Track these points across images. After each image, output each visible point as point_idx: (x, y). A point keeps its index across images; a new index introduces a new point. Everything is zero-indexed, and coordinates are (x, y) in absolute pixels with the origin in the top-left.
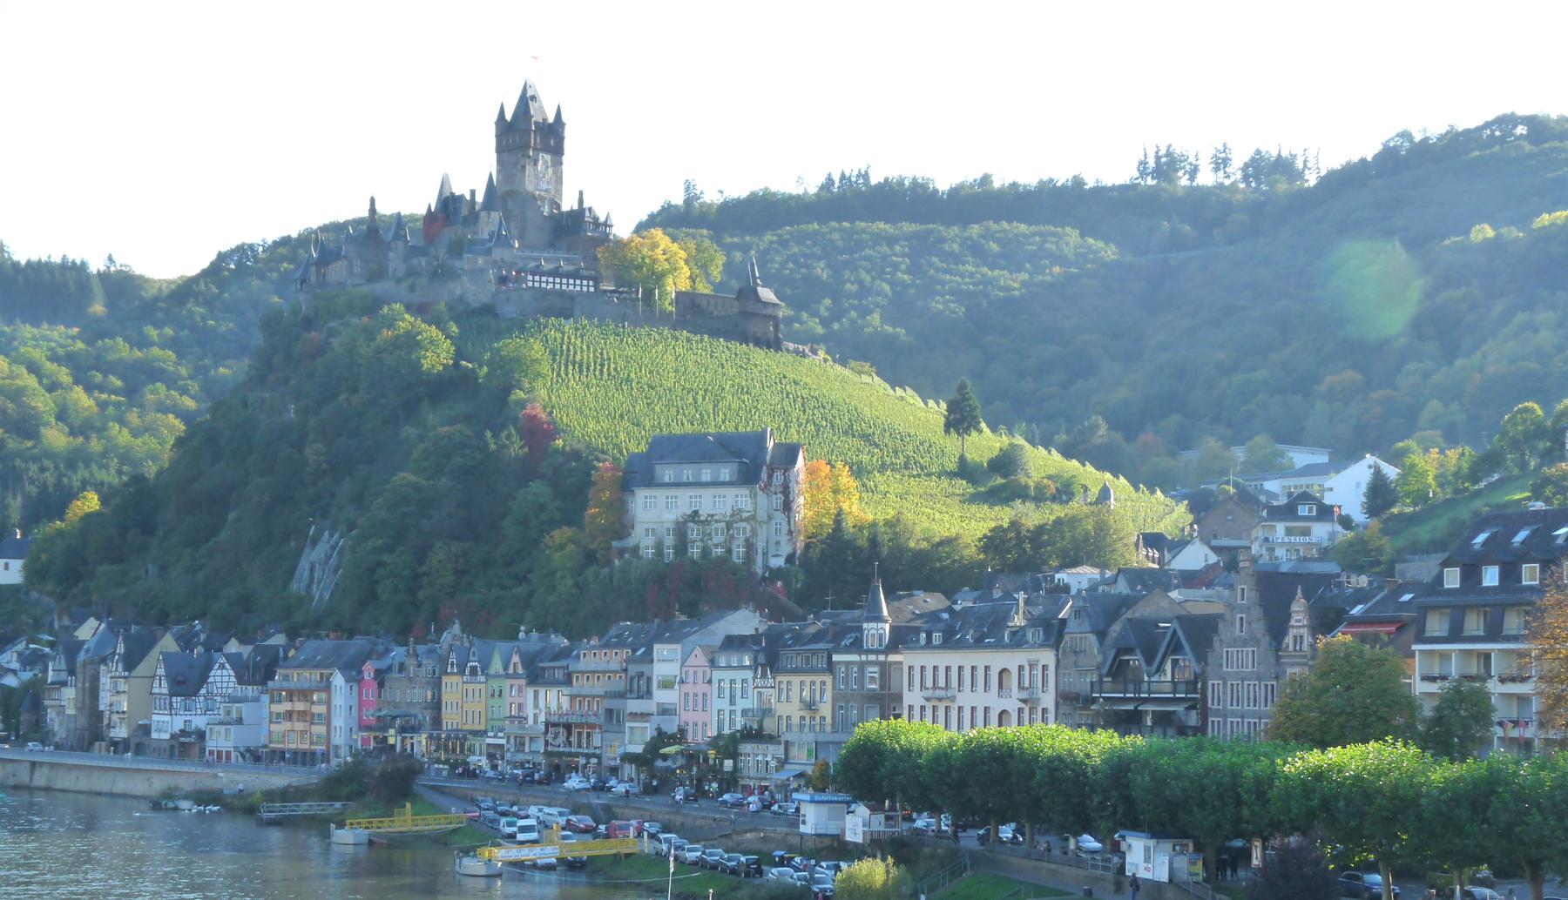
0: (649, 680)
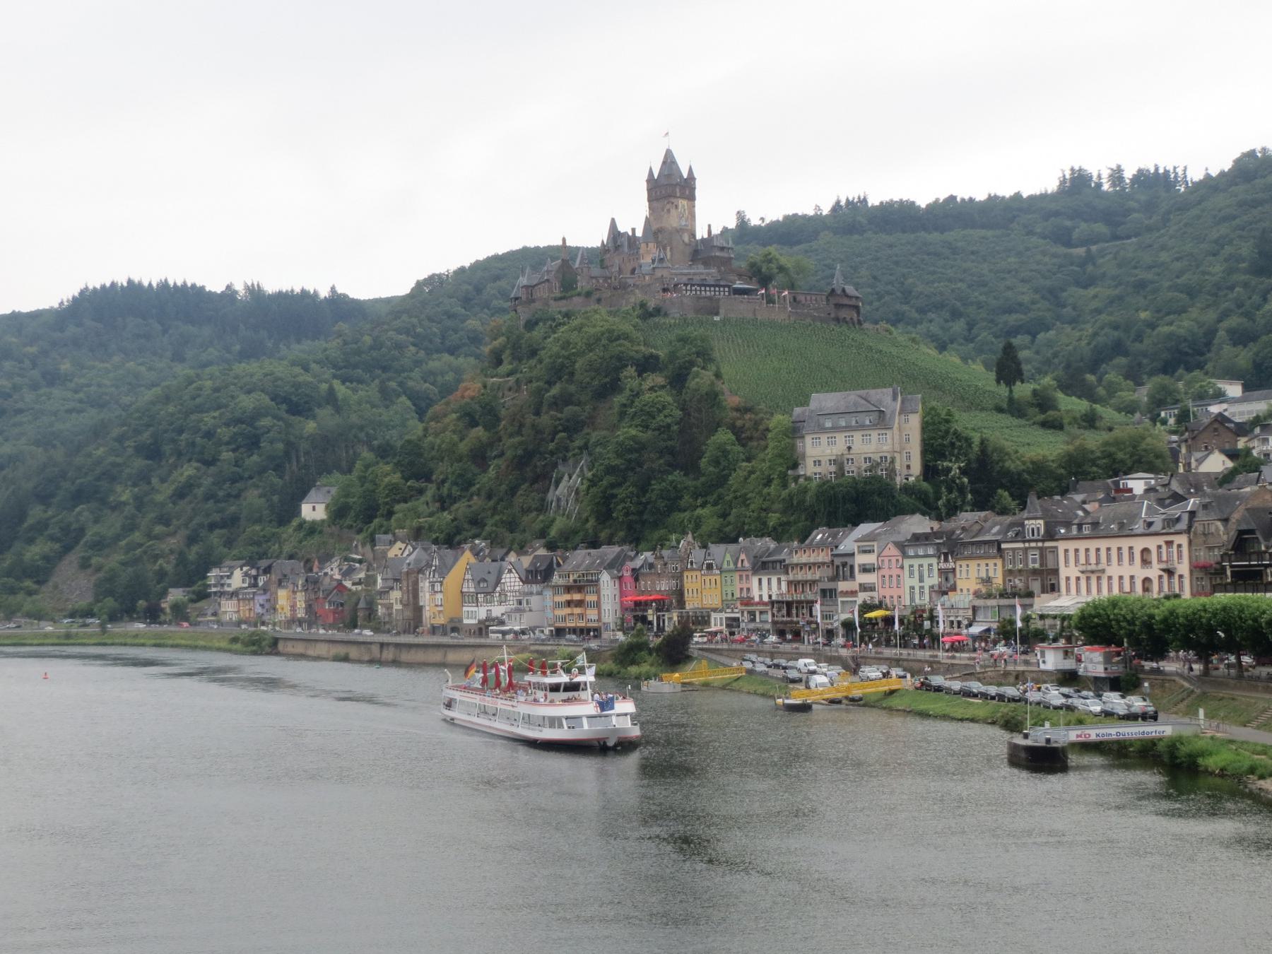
0: (852, 567)
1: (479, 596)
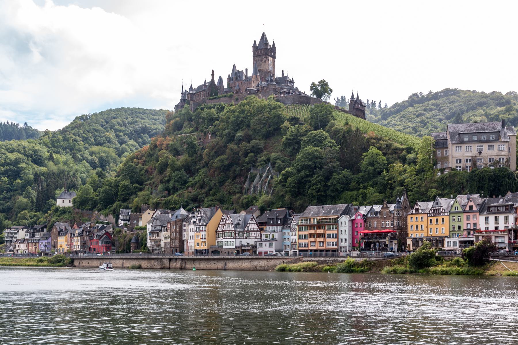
1: (236, 232)
